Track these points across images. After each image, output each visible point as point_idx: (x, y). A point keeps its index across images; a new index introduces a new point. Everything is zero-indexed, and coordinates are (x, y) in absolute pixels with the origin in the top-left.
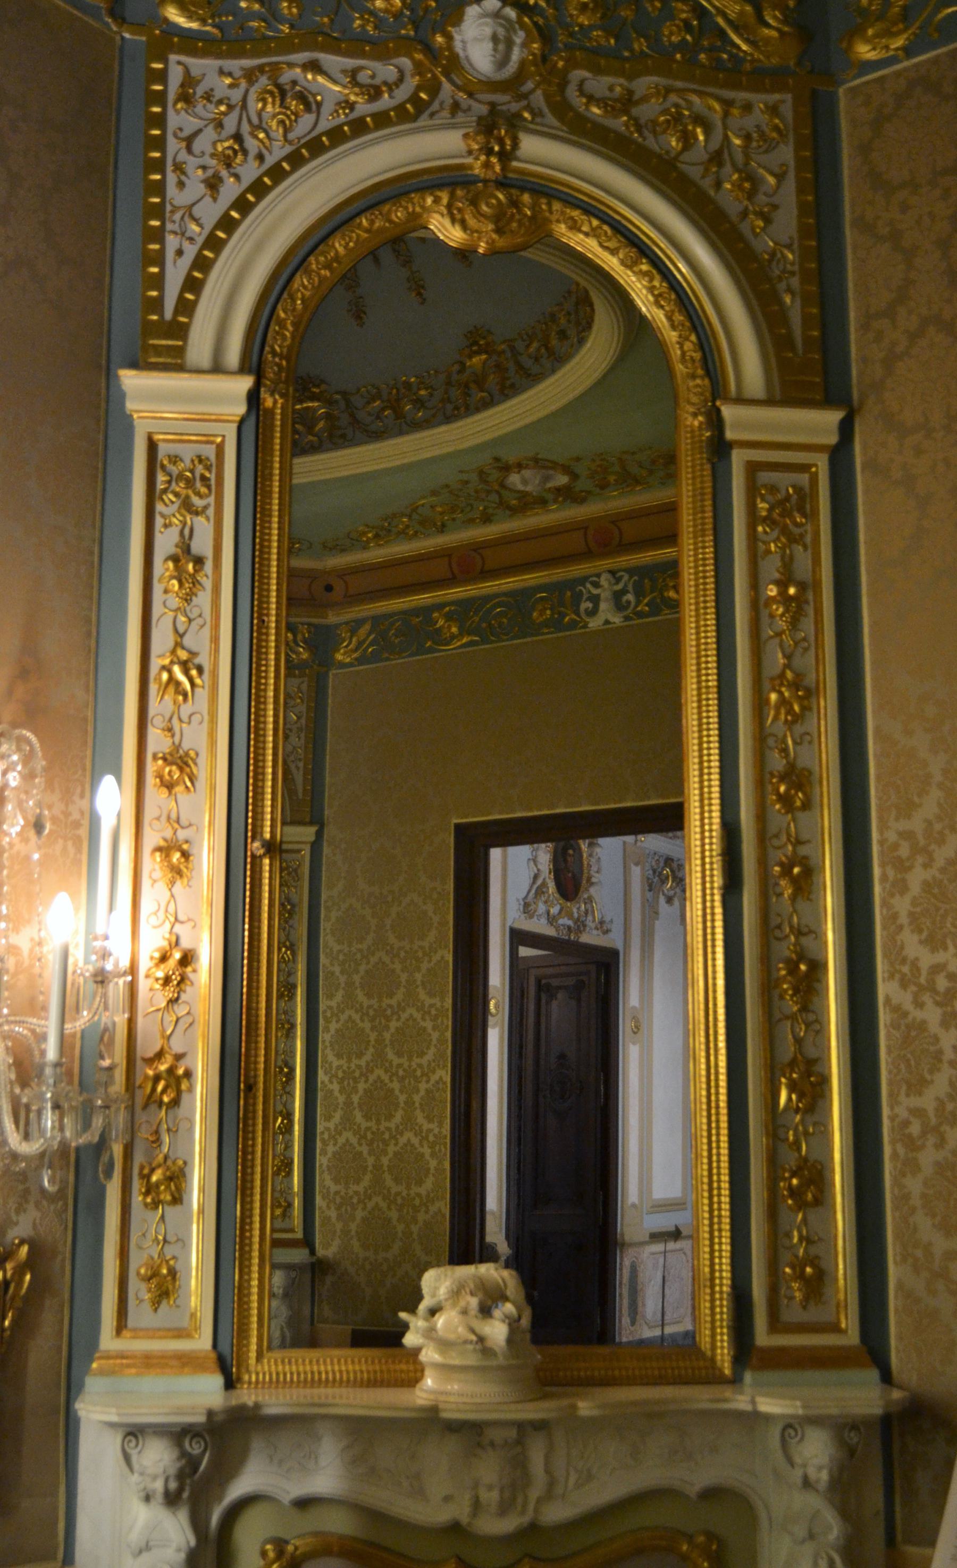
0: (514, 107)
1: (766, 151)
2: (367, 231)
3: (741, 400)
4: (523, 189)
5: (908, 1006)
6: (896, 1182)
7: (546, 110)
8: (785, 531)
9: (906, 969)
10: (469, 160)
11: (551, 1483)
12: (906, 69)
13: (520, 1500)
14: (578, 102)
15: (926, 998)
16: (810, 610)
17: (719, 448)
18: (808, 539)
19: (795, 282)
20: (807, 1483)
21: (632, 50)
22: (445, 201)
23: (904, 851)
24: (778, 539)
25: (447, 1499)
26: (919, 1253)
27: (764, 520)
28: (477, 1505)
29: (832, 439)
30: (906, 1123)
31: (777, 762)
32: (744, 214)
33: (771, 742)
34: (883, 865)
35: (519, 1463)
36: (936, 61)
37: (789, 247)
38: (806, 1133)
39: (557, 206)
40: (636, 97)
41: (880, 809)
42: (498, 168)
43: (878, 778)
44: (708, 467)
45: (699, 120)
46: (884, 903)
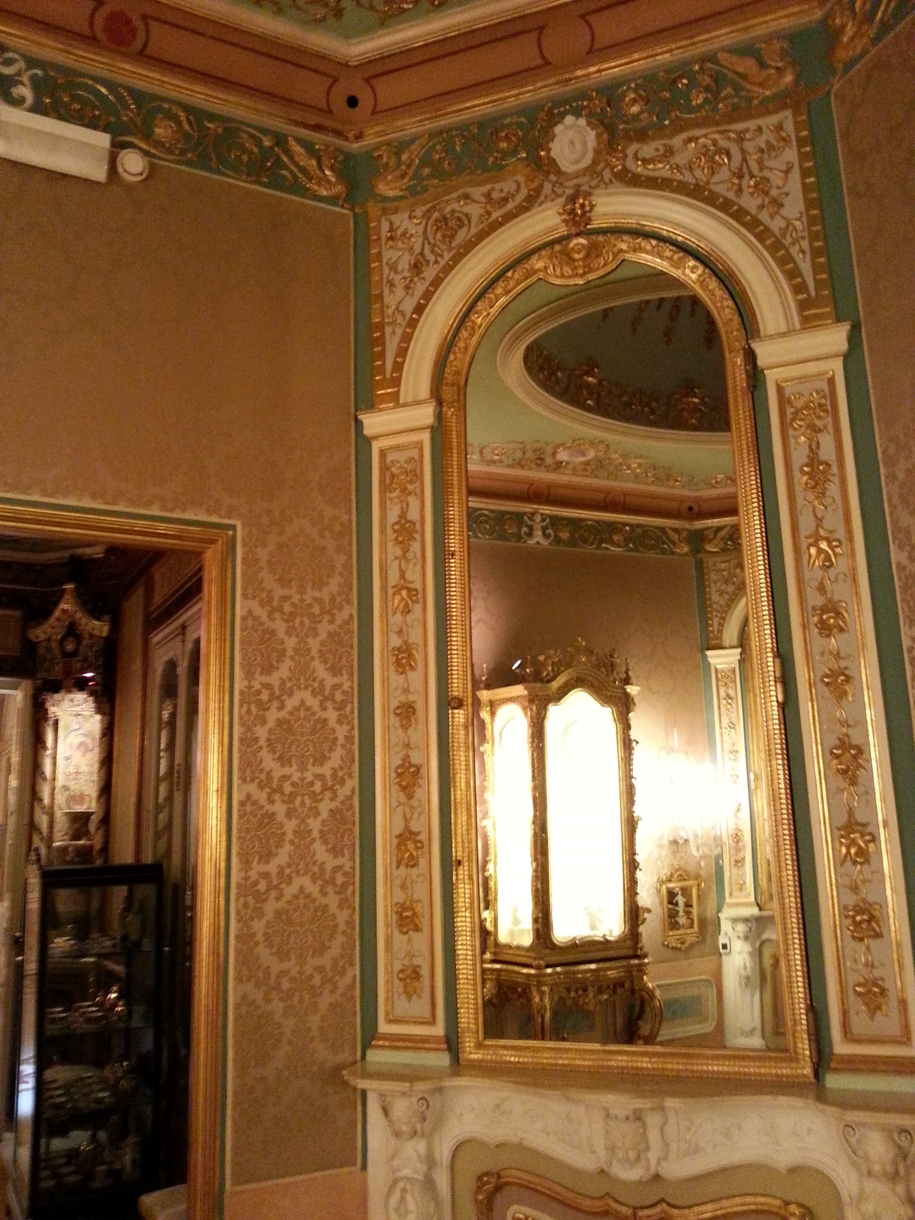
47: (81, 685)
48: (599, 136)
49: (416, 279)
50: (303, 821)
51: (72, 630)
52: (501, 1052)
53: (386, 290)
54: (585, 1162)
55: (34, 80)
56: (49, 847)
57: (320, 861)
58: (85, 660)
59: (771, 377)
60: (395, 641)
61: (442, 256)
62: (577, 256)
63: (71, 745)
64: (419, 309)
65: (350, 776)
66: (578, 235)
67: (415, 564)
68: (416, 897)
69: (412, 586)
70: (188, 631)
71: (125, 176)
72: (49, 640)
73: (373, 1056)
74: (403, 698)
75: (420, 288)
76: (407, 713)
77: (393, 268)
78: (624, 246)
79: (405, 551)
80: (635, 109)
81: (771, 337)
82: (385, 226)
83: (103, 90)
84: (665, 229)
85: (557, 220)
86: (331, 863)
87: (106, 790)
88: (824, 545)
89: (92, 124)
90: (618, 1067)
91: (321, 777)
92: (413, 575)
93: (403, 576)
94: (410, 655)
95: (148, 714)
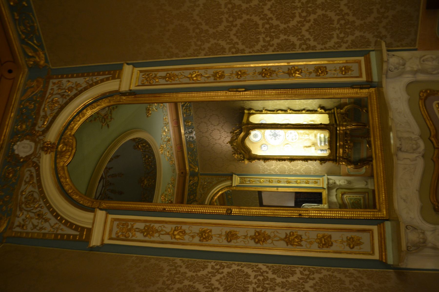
48: (27, 139)
49: (44, 217)
50: (277, 284)
52: (381, 200)
53: (43, 231)
54: (420, 163)
57: (298, 279)
59: (133, 88)
60: (197, 240)
61: (40, 205)
62: (64, 149)
64: (57, 216)
65: (257, 266)
66: (57, 148)
67: (164, 227)
68: (316, 238)
69: (173, 229)
73: (390, 261)
74: (224, 238)
75: (49, 216)
76: (231, 236)
77: (35, 227)
78: (69, 133)
79: (157, 231)
80: (24, 127)
81: (120, 87)
82: (18, 229)
84: (70, 118)
85: (48, 156)
86: (298, 275)
88: (194, 75)
90: (381, 153)
91: (256, 277)
92: (169, 228)
93: (168, 234)
94: (204, 232)
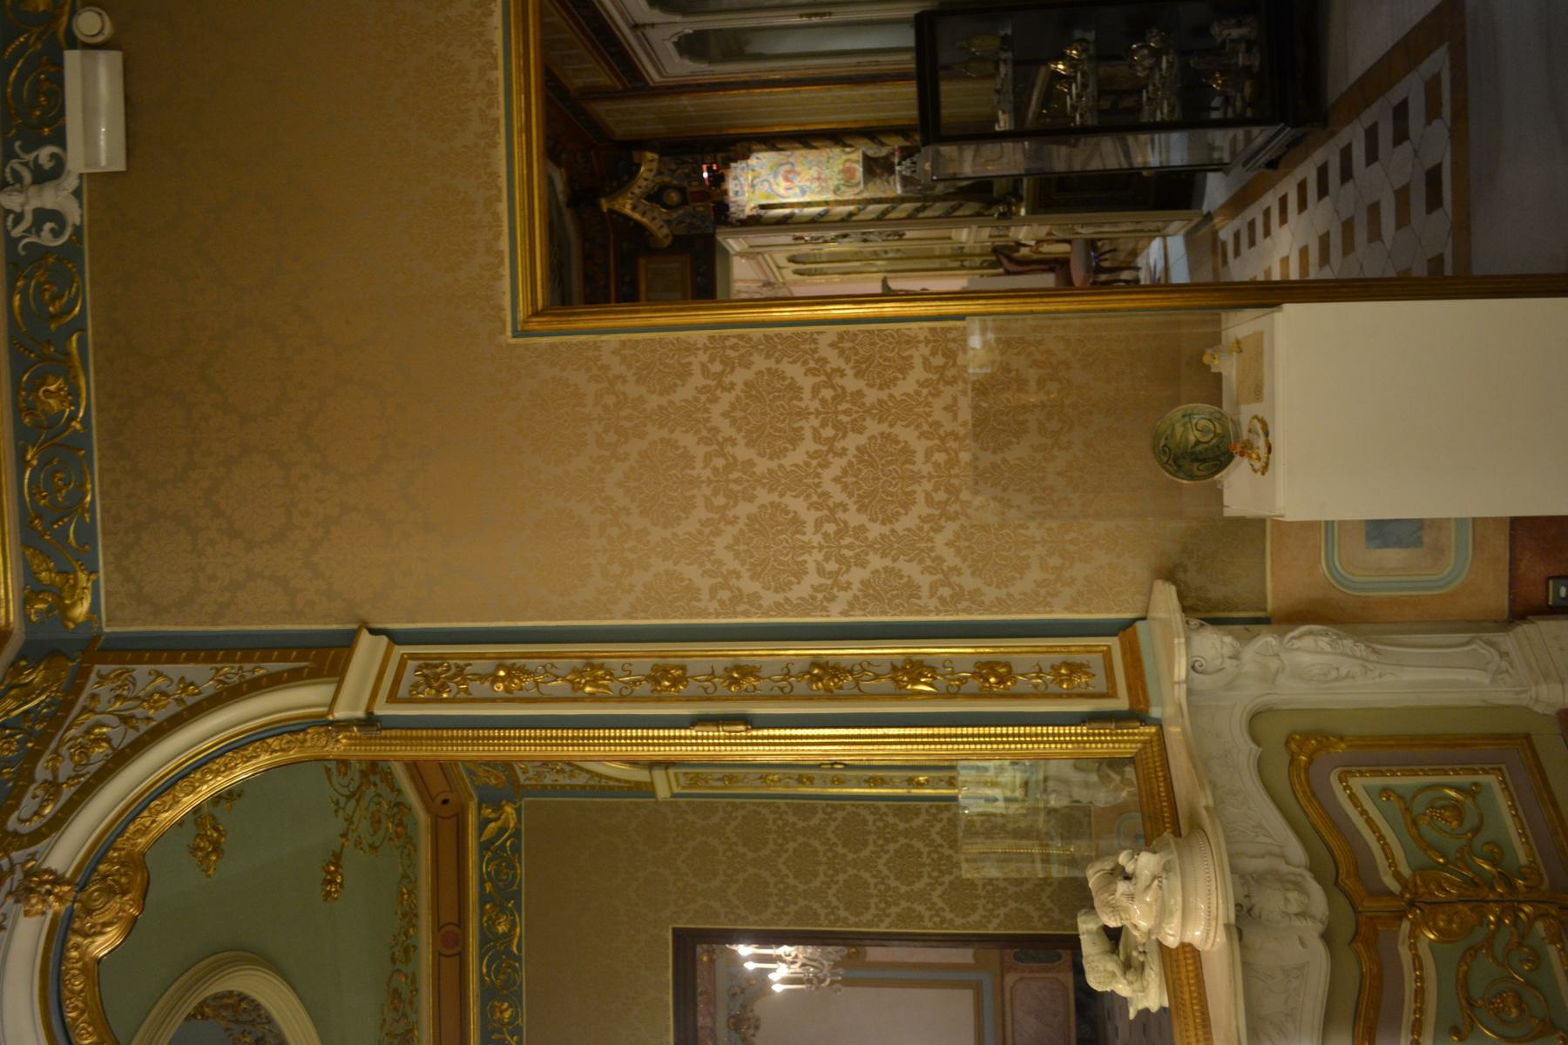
0: (18, 875)
1: (134, 684)
2: (82, 1013)
3: (332, 705)
4: (95, 869)
5: (848, 595)
6: (988, 611)
7: (32, 849)
8: (450, 679)
9: (820, 596)
10: (50, 914)
11: (1271, 854)
12: (106, 573)
13: (1292, 878)
14: (36, 823)
15: (843, 579)
16: (519, 662)
17: (370, 722)
18: (462, 663)
19: (247, 666)
20: (1235, 657)
21: (9, 780)
22: (80, 939)
23: (725, 595)
24: (458, 684)
25: (1303, 944)
26: (1043, 591)
27: (439, 691)
28: (1303, 915)
29: (384, 640)
30: (942, 599)
31: (646, 687)
32: (180, 701)
33: (625, 692)
34: (736, 615)
35: (1260, 878)
36: (106, 547)
37: (218, 670)
38: (953, 673)
39: (119, 842)
40: (50, 778)
41: (691, 615)
42: (66, 888)
43: (665, 616)
44: (383, 733)
45: (88, 732)
46: (766, 614)
47: (718, 179)
51: (655, 197)
55: (27, 149)
56: (902, 200)
58: (688, 176)
63: (788, 189)
70: (640, 19)
71: (108, 31)
72: (668, 222)
83: (14, 74)
87: (837, 137)
89: (58, 80)
95: (744, 77)
